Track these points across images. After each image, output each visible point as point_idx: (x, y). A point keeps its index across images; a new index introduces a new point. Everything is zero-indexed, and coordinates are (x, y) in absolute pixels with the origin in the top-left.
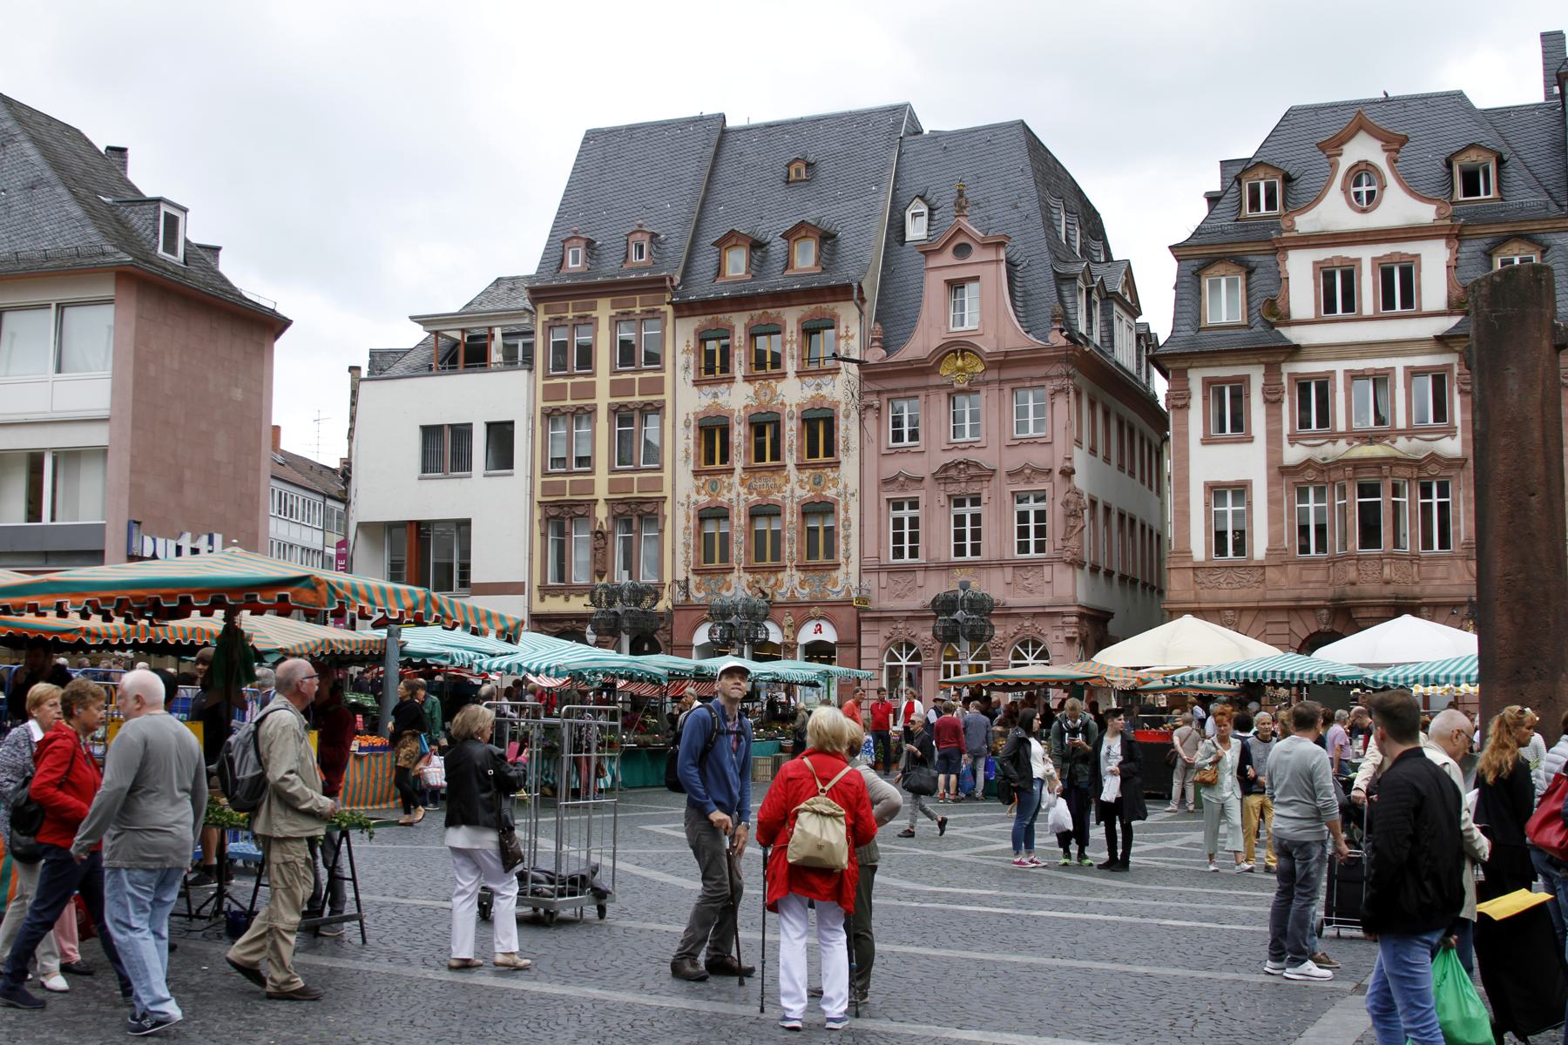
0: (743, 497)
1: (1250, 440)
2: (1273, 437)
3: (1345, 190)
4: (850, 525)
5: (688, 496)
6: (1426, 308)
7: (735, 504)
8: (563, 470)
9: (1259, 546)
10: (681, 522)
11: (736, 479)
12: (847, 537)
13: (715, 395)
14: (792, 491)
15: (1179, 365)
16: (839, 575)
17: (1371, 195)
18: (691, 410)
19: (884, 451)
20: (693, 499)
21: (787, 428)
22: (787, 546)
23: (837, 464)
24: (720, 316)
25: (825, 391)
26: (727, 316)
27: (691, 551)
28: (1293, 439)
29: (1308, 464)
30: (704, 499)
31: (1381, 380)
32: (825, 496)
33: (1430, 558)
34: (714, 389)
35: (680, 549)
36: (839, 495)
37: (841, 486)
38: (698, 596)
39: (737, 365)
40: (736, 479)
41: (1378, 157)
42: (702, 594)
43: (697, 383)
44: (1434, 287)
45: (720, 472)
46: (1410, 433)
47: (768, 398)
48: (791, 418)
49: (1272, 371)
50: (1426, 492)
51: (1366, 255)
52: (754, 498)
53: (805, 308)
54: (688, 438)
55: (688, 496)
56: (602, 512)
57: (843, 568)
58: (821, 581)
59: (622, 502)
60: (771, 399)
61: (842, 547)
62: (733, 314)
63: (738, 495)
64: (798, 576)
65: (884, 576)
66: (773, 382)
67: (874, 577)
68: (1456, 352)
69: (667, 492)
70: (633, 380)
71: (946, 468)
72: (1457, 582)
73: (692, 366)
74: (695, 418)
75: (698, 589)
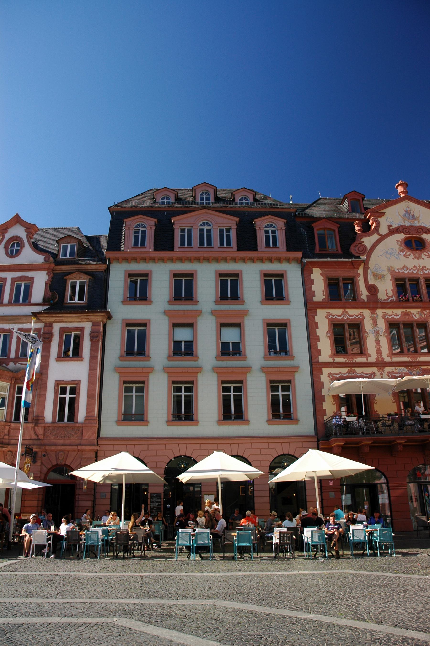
3: (6, 247)
68: (43, 322)
72: (28, 438)
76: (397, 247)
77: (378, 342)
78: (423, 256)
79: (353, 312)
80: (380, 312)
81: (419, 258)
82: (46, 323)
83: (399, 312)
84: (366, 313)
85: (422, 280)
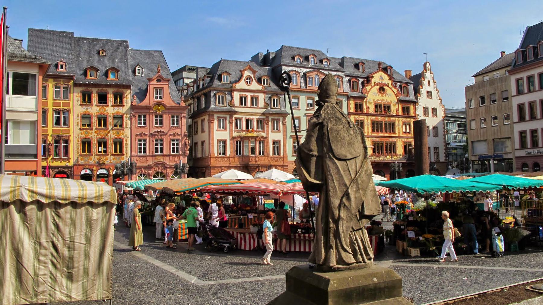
0: (95, 136)
1: (227, 131)
2: (231, 130)
4: (127, 145)
5: (78, 135)
6: (260, 107)
7: (93, 138)
8: (66, 126)
9: (228, 154)
10: (76, 142)
11: (94, 131)
12: (126, 148)
13: (87, 109)
14: (111, 135)
15: (212, 113)
16: (125, 157)
17: (250, 82)
18: (79, 112)
19: (137, 127)
20: (80, 136)
21: (109, 119)
22: (109, 149)
23: (123, 130)
24: (89, 88)
25: (120, 111)
26: (91, 88)
27: (79, 150)
28: (235, 131)
29: (239, 137)
30: (83, 136)
31: (252, 120)
32: (120, 137)
33: (261, 157)
34: (87, 107)
35: (75, 149)
36: (124, 137)
37: (125, 135)
38: (81, 162)
39: (94, 102)
40: (94, 131)
41: (252, 76)
42: (83, 161)
43: (81, 105)
44: (261, 104)
45: (88, 129)
46: (256, 131)
47: (103, 111)
48: (110, 117)
49: (231, 117)
50: (260, 143)
51: (249, 95)
52: (99, 136)
53: (115, 89)
54: (78, 119)
55: (78, 135)
56: (50, 139)
57: (125, 155)
58: (119, 158)
59: (58, 136)
60: (104, 111)
61: (125, 150)
62: (93, 88)
63: (94, 135)
64: (112, 157)
65: (138, 158)
66: (105, 107)
67: (135, 158)
69: (71, 133)
70: (60, 102)
71: (155, 132)
73: (79, 100)
74: (80, 115)
75: (81, 160)
76: (376, 91)
77: (368, 128)
78: (384, 96)
79: (362, 117)
80: (369, 117)
81: (382, 96)
82: (266, 116)
83: (375, 117)
84: (365, 117)
85: (383, 105)
